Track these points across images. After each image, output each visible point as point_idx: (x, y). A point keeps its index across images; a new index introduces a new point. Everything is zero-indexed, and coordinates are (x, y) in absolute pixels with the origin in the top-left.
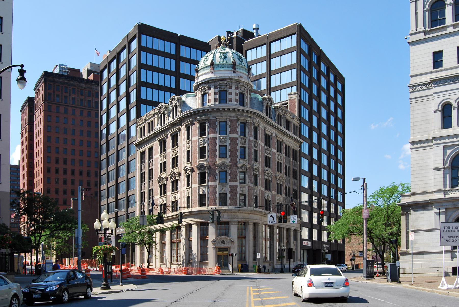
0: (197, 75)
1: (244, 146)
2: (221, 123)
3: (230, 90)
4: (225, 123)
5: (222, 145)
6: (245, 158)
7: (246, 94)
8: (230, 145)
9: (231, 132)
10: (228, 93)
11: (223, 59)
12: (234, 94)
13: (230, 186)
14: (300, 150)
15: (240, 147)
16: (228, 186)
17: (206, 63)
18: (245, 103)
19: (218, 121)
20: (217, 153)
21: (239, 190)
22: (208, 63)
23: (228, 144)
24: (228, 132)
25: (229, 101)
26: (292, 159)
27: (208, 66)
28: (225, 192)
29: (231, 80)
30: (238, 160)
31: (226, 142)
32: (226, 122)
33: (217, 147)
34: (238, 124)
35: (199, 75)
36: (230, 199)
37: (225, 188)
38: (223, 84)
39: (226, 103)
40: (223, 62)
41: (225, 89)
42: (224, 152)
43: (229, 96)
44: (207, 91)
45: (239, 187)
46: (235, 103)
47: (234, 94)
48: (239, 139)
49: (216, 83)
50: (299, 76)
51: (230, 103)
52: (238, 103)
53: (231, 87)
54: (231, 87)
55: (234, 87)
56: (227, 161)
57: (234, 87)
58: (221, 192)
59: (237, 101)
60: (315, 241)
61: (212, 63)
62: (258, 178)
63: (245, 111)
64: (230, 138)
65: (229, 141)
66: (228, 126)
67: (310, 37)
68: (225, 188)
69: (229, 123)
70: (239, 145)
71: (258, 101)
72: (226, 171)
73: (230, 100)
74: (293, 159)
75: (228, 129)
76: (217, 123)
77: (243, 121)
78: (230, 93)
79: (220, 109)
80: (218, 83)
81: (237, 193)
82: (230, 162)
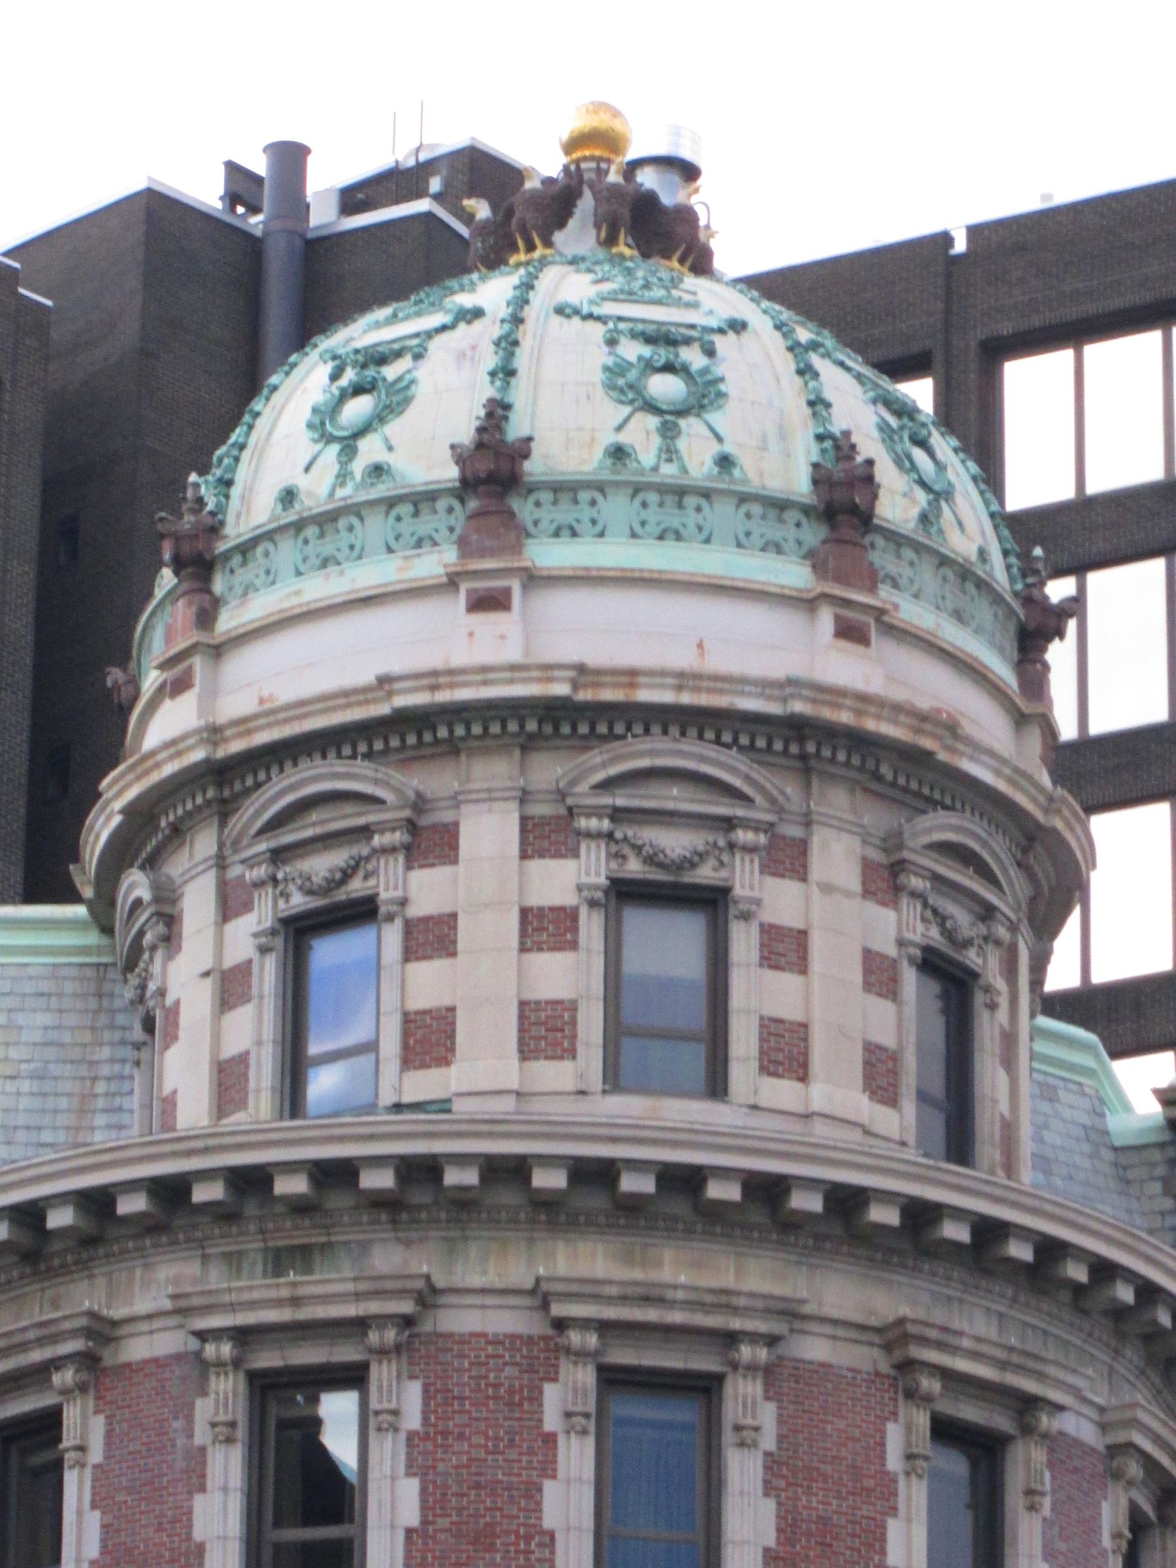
0: (206, 618)
3: (781, 901)
4: (681, 1412)
10: (744, 943)
11: (670, 418)
12: (834, 961)
17: (370, 449)
18: (986, 1126)
19: (586, 1376)
22: (425, 443)
25: (770, 1066)
27: (422, 500)
29: (807, 741)
32: (705, 1389)
34: (901, 1436)
35: (228, 622)
38: (675, 797)
39: (716, 1086)
40: (670, 453)
41: (706, 874)
43: (757, 993)
44: (388, 881)
46: (858, 1103)
47: (834, 961)
49: (549, 770)
51: (782, 1092)
52: (898, 1122)
53: (789, 858)
54: (789, 858)
57: (837, 856)
59: (879, 1073)
61: (494, 472)
66: (743, 1471)
71: (1097, 1135)
73: (787, 1052)
76: (566, 1393)
77: (970, 1412)
78: (787, 949)
79: (632, 1183)
80: (602, 763)
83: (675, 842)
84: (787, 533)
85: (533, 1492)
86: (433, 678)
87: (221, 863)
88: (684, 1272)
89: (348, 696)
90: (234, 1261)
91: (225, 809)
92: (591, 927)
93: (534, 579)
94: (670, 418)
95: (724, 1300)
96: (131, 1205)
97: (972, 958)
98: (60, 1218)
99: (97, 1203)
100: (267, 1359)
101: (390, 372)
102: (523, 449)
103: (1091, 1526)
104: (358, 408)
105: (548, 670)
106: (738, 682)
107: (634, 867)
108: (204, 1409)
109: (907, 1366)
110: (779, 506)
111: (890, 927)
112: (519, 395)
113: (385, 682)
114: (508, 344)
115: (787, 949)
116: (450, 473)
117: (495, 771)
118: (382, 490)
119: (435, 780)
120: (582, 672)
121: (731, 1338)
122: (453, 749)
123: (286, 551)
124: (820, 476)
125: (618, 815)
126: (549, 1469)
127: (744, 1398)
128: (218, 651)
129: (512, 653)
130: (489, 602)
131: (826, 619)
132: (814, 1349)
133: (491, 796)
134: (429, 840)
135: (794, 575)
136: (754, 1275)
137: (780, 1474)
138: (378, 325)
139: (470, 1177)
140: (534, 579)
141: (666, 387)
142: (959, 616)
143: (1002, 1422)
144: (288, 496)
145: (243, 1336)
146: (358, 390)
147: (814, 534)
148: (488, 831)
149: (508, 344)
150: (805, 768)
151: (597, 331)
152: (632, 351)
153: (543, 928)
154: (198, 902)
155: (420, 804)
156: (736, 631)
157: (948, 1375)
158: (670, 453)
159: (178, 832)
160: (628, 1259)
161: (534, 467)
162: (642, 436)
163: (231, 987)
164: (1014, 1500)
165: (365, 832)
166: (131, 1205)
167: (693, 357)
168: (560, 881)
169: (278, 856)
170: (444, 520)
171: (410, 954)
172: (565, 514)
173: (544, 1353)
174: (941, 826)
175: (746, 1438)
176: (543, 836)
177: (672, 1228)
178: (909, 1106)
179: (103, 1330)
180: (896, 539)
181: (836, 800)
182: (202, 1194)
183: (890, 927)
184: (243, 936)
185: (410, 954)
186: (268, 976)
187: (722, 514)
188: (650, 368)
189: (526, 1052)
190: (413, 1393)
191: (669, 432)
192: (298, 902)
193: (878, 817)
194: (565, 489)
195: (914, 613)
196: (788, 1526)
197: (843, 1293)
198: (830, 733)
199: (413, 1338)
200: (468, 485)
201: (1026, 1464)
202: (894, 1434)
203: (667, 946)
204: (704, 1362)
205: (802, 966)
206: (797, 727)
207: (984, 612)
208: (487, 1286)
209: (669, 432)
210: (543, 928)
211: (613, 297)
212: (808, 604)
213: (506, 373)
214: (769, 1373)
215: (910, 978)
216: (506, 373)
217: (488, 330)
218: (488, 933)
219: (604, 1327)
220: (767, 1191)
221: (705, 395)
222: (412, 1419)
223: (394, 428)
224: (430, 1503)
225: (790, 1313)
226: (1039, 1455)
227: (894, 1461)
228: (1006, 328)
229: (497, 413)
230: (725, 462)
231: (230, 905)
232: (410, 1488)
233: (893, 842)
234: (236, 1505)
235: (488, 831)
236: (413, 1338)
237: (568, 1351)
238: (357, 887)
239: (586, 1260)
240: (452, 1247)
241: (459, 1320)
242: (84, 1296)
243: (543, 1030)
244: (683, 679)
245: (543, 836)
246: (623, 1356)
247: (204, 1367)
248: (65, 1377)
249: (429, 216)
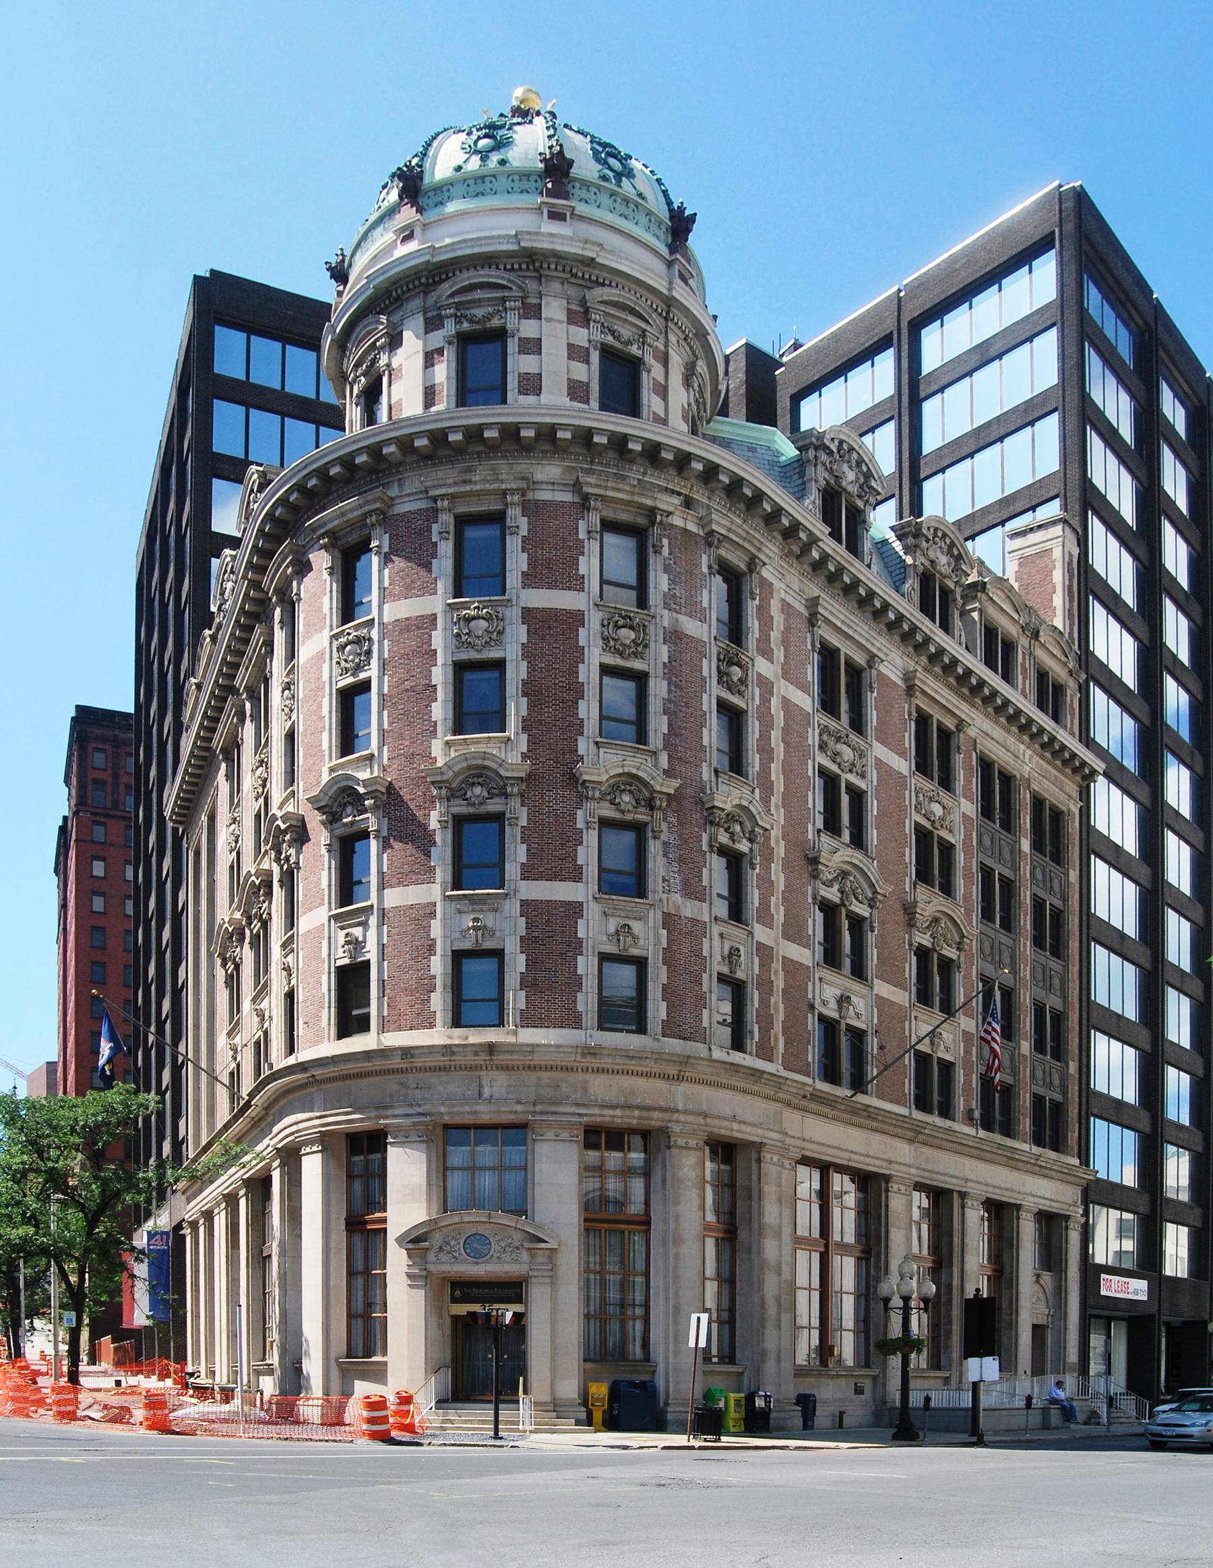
1: (637, 665)
2: (472, 533)
3: (529, 328)
5: (472, 655)
6: (642, 737)
7: (649, 359)
8: (528, 652)
9: (530, 580)
10: (512, 346)
13: (525, 904)
14: (1085, 812)
15: (606, 670)
16: (512, 908)
20: (440, 710)
21: (595, 929)
23: (512, 647)
24: (513, 580)
25: (523, 391)
26: (1026, 845)
28: (489, 944)
29: (532, 262)
30: (583, 746)
31: (497, 636)
32: (498, 518)
33: (440, 675)
36: (526, 983)
37: (489, 920)
38: (479, 294)
39: (504, 401)
41: (495, 322)
42: (496, 706)
43: (519, 364)
45: (593, 910)
48: (594, 619)
50: (1074, 454)
53: (533, 312)
54: (533, 312)
55: (554, 308)
56: (508, 748)
57: (554, 308)
58: (467, 945)
60: (1174, 1280)
62: (752, 878)
64: (529, 615)
65: (517, 635)
66: (513, 544)
67: (1146, 290)
68: (489, 920)
69: (519, 521)
70: (595, 656)
72: (499, 818)
73: (532, 384)
74: (1037, 846)
75: (517, 562)
77: (624, 516)
78: (532, 346)
79: (455, 437)
80: (447, 288)
81: (577, 946)
82: (524, 757)
121: (504, 493)
125: (458, 306)
134: (395, 341)
196: (532, 563)
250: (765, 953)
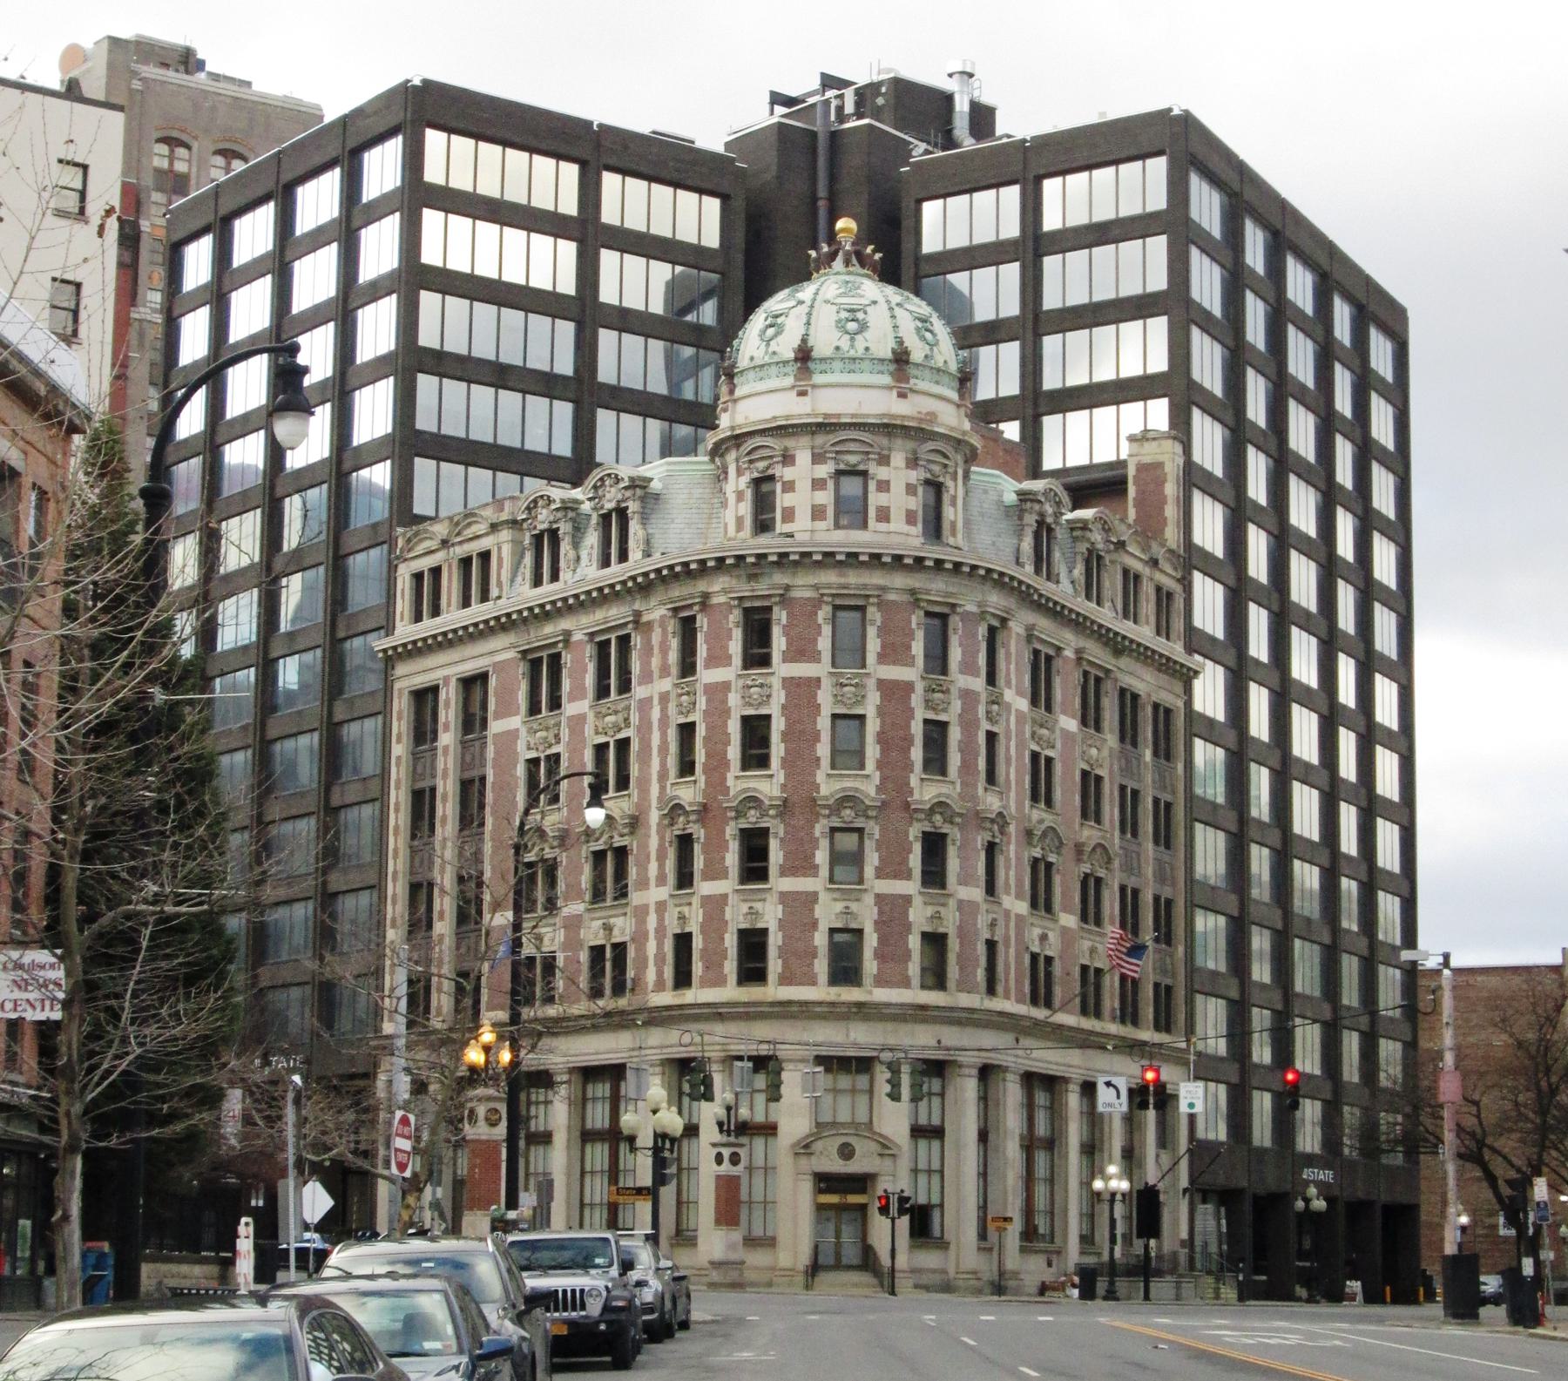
0: (732, 392)
1: (943, 717)
2: (841, 614)
3: (881, 473)
4: (856, 615)
5: (843, 711)
6: (943, 772)
7: (950, 483)
8: (881, 712)
9: (883, 658)
10: (872, 486)
11: (853, 336)
12: (898, 488)
13: (878, 896)
15: (926, 721)
16: (869, 899)
17: (773, 346)
18: (946, 526)
19: (829, 609)
20: (823, 750)
21: (919, 916)
22: (786, 347)
23: (870, 709)
24: (871, 658)
25: (879, 519)
27: (785, 363)
28: (854, 926)
29: (890, 429)
30: (914, 781)
31: (861, 699)
32: (862, 609)
33: (824, 723)
34: (916, 619)
35: (738, 393)
36: (879, 955)
37: (854, 906)
38: (852, 447)
39: (864, 525)
40: (852, 346)
41: (861, 467)
42: (855, 746)
43: (876, 499)
44: (778, 471)
45: (917, 901)
46: (906, 528)
47: (898, 488)
48: (920, 687)
49: (820, 440)
50: (1180, 351)
51: (883, 526)
52: (918, 529)
53: (884, 460)
54: (884, 460)
55: (898, 459)
56: (868, 784)
57: (898, 459)
59: (910, 518)
61: (804, 355)
62: (1000, 861)
63: (949, 566)
64: (882, 684)
65: (873, 699)
66: (872, 632)
68: (854, 906)
70: (920, 714)
71: (1000, 502)
72: (860, 831)
73: (884, 515)
75: (873, 645)
76: (823, 613)
77: (937, 609)
78: (884, 486)
80: (833, 438)
81: (908, 927)
82: (879, 789)
83: (853, 459)
84: (884, 368)
85: (816, 640)
86: (787, 417)
87: (737, 460)
88: (854, 578)
89: (766, 421)
90: (738, 577)
91: (738, 446)
92: (831, 484)
93: (814, 386)
94: (853, 336)
95: (865, 587)
96: (711, 564)
97: (941, 479)
98: (693, 566)
99: (703, 562)
100: (748, 604)
101: (779, 320)
102: (811, 350)
103: (975, 635)
104: (771, 331)
105: (816, 415)
106: (868, 416)
107: (842, 467)
108: (731, 618)
109: (917, 600)
110: (882, 360)
111: (914, 476)
112: (812, 332)
113: (775, 418)
114: (809, 314)
115: (884, 486)
116: (792, 355)
117: (805, 441)
118: (776, 359)
119: (790, 443)
120: (826, 415)
121: (868, 596)
122: (793, 434)
123: (751, 375)
124: (894, 351)
125: (837, 452)
126: (819, 634)
127: (873, 613)
128: (735, 401)
129: (809, 411)
130: (802, 394)
131: (895, 393)
132: (892, 597)
133: (804, 447)
135: (887, 380)
136: (876, 578)
137: (883, 631)
138: (782, 301)
139: (797, 557)
140: (814, 386)
141: (852, 326)
142: (937, 383)
143: (946, 610)
144: (752, 359)
145: (740, 599)
146: (771, 326)
147: (892, 367)
148: (803, 457)
149: (809, 314)
150: (889, 435)
151: (835, 308)
152: (844, 315)
153: (818, 484)
154: (732, 470)
155: (786, 449)
156: (870, 399)
157: (929, 602)
158: (852, 346)
159: (727, 449)
160: (840, 576)
161: (815, 354)
162: (845, 343)
163: (740, 496)
164: (950, 631)
165: (771, 457)
166: (711, 564)
167: (860, 315)
168: (824, 470)
169: (751, 462)
170: (792, 369)
171: (783, 491)
172: (823, 366)
173: (817, 603)
174: (931, 445)
175: (873, 622)
176: (817, 458)
177: (851, 566)
178: (920, 526)
179: (706, 596)
180: (918, 365)
181: (899, 442)
182: (729, 561)
183: (914, 476)
184: (744, 480)
185: (783, 491)
186: (749, 494)
187: (866, 365)
188: (848, 320)
189: (813, 519)
190: (784, 613)
191: (852, 339)
192: (756, 475)
193: (910, 445)
194: (823, 360)
195: (922, 385)
196: (883, 647)
197: (900, 580)
198: (895, 426)
199: (784, 600)
200: (796, 360)
201: (955, 621)
202: (914, 619)
203: (851, 486)
204: (860, 602)
205: (888, 490)
206: (886, 426)
207: (946, 379)
208: (803, 585)
209: (852, 339)
210: (818, 484)
211: (840, 295)
212: (890, 388)
213: (808, 323)
214: (879, 605)
215: (920, 490)
216: (808, 323)
217: (804, 309)
218: (803, 486)
219: (833, 595)
220: (876, 557)
221: (864, 327)
222: (784, 621)
223: (780, 338)
224: (789, 644)
225: (884, 589)
226: (957, 618)
227: (914, 626)
228: (1042, 172)
229: (804, 341)
230: (867, 349)
231: (739, 473)
232: (784, 639)
233: (915, 452)
234: (740, 644)
235: (803, 457)
236: (784, 600)
237: (390, 1099)
238: (770, 472)
239: (829, 577)
240: (794, 574)
241: (796, 594)
242: (702, 586)
243: (818, 513)
244: (853, 416)
245: (817, 458)
246: (838, 602)
247: (732, 607)
248: (696, 608)
249: (870, 126)
250: (1007, 913)
